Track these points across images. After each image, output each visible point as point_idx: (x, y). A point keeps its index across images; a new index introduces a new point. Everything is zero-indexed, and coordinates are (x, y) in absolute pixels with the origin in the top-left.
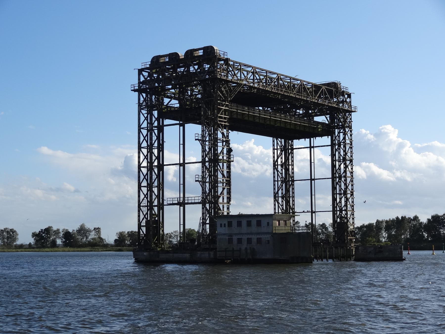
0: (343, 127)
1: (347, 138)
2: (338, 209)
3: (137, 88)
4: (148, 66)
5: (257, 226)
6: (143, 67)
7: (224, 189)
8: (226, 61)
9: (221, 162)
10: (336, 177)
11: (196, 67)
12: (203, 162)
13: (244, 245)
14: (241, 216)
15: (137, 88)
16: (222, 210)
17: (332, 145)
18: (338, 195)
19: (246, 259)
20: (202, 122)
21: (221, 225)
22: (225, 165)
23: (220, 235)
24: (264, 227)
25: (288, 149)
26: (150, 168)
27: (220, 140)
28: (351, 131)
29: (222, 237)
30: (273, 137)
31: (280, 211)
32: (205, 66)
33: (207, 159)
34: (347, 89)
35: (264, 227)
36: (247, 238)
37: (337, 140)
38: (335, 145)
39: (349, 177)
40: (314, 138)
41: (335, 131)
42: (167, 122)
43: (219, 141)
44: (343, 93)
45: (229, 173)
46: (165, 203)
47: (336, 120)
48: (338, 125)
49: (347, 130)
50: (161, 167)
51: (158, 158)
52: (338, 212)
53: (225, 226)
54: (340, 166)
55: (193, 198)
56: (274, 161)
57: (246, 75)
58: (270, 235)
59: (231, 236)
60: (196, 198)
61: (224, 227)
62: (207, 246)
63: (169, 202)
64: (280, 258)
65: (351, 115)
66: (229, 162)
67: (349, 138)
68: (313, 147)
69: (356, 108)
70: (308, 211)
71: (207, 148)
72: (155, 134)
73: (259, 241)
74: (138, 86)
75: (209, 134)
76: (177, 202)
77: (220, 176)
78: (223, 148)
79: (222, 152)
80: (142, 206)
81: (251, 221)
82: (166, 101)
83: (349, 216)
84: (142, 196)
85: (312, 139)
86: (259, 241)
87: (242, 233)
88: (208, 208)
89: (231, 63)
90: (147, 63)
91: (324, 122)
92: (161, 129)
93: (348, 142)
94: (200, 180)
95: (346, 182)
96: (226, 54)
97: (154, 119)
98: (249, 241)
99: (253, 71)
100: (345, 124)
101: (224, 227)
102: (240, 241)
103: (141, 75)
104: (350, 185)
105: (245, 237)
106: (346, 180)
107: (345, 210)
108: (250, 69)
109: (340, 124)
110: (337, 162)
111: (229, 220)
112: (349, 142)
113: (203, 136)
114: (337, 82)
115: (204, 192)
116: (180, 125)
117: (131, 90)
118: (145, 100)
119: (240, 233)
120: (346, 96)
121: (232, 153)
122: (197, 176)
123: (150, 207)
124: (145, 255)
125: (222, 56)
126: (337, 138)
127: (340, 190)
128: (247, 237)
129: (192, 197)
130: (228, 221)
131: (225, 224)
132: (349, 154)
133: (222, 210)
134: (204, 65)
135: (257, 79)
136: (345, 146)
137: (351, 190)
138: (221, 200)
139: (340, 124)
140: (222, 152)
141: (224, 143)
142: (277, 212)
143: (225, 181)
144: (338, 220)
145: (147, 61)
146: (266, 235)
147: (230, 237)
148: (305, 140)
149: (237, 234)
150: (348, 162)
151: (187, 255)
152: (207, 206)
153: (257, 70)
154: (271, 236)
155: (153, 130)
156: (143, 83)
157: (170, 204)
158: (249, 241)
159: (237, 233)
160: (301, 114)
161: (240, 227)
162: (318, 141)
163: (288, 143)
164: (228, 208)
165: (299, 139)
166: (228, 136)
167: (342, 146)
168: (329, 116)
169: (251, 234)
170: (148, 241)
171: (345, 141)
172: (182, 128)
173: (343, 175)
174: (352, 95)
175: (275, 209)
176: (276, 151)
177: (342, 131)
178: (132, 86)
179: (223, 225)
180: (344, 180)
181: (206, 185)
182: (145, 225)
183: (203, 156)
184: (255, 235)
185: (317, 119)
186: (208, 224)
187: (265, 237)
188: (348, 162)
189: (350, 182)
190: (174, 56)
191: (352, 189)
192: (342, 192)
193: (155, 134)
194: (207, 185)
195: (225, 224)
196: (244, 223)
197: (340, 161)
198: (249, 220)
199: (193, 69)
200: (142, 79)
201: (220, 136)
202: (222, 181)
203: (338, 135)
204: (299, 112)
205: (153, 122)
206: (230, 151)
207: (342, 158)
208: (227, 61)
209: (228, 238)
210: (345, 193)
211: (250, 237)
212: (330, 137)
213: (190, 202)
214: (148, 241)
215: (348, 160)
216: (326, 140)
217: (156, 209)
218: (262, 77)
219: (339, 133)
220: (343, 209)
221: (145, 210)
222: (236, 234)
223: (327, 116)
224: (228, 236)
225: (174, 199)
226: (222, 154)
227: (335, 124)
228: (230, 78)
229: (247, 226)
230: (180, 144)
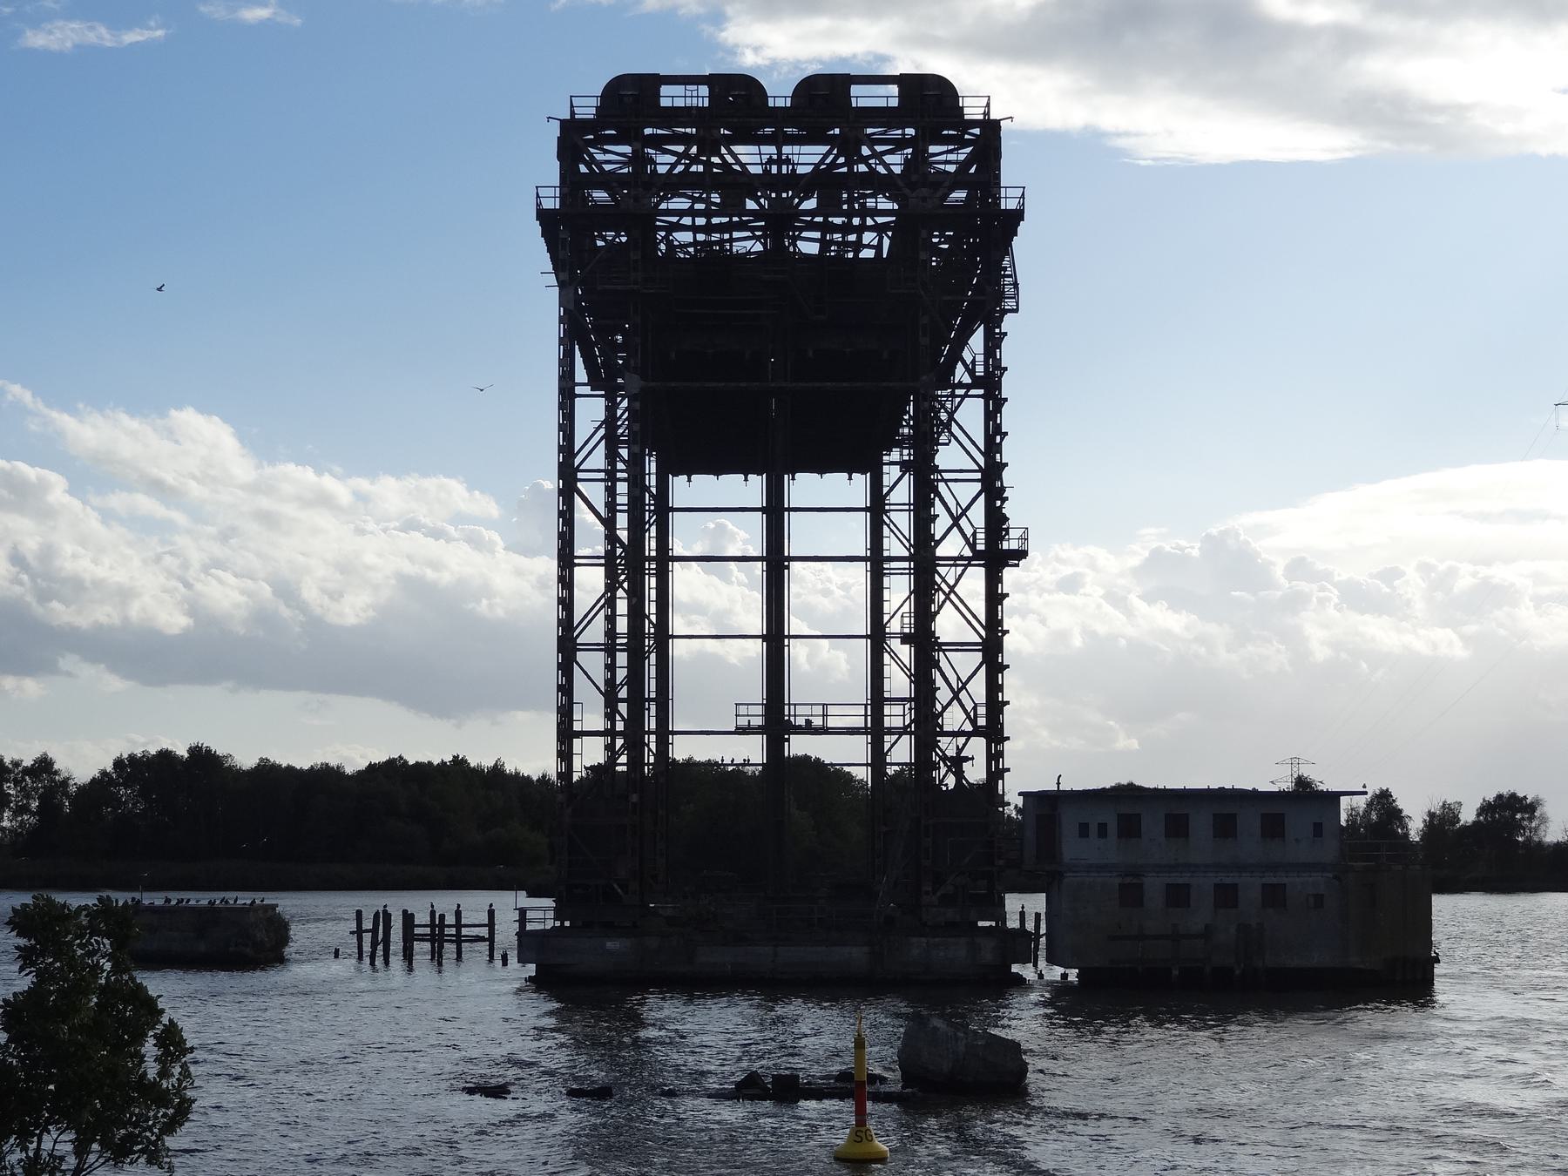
19: (1237, 972)
21: (1084, 830)
24: (1297, 840)
35: (1297, 840)
36: (1215, 884)
58: (1330, 875)
63: (743, 722)
64: (1362, 966)
70: (733, 760)
73: (1274, 896)
81: (1234, 816)
86: (1274, 896)
98: (1226, 896)
102: (1178, 896)
128: (1217, 881)
129: (812, 705)
131: (1103, 830)
147: (1128, 880)
151: (855, 954)
154: (1335, 877)
158: (1226, 896)
165: (717, 473)
170: (619, 890)
179: (1093, 829)
184: (1254, 875)
196: (1201, 824)
211: (1228, 881)
214: (616, 886)
229: (1215, 837)
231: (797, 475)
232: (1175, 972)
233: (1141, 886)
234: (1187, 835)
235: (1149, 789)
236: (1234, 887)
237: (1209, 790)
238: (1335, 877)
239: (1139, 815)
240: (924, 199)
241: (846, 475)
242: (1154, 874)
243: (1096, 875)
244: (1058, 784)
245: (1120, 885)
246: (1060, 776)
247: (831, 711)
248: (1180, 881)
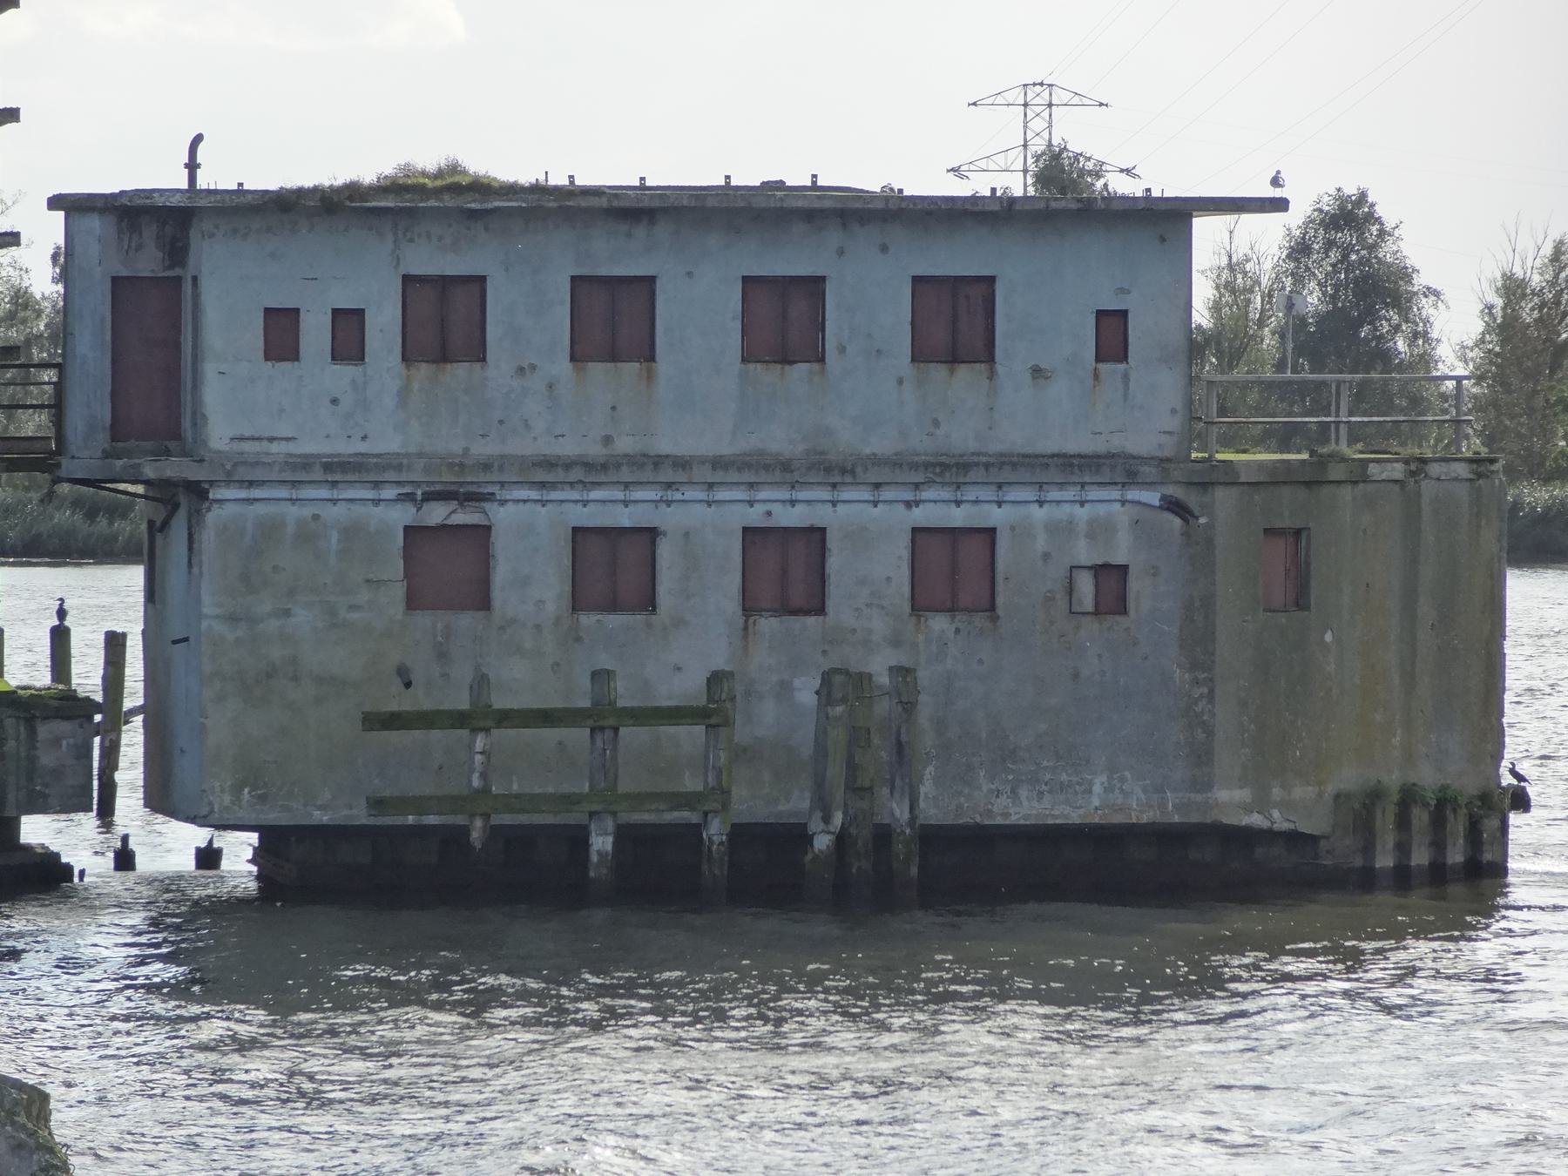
19: (822, 842)
23: (251, 484)
24: (1037, 372)
29: (307, 511)
35: (1037, 372)
36: (750, 534)
58: (1153, 497)
61: (337, 356)
64: (1256, 820)
81: (815, 286)
87: (658, 461)
101: (337, 356)
111: (428, 260)
119: (624, 445)
128: (755, 516)
130: (407, 279)
146: (1070, 493)
147: (437, 514)
159: (568, 448)
179: (315, 333)
184: (887, 494)
224: (409, 497)
232: (602, 842)
233: (482, 533)
234: (648, 355)
235: (512, 190)
237: (727, 189)
238: (1174, 506)
239: (478, 282)
242: (534, 495)
243: (324, 493)
244: (192, 166)
245: (407, 529)
246: (198, 139)
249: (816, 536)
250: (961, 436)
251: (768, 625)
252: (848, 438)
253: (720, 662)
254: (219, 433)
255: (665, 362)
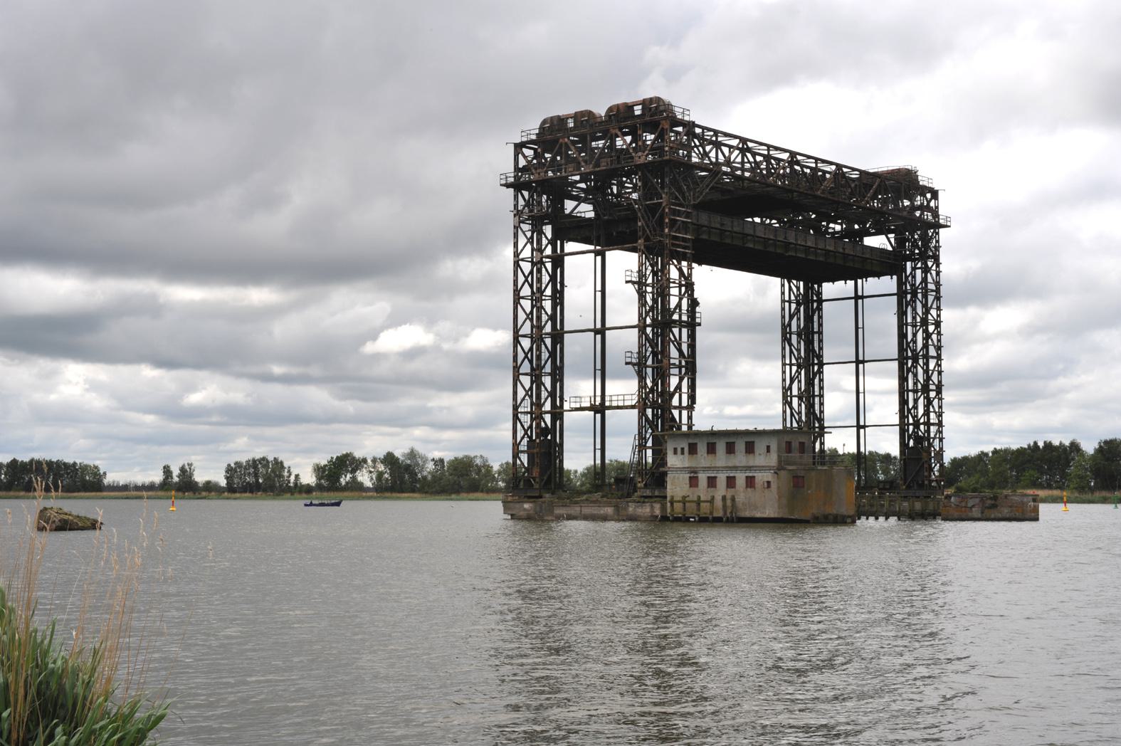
0: (924, 257)
1: (930, 279)
2: (911, 421)
3: (512, 180)
4: (534, 137)
5: (746, 452)
6: (524, 139)
7: (681, 379)
8: (687, 128)
9: (676, 327)
10: (908, 358)
11: (628, 139)
12: (641, 327)
13: (721, 489)
14: (712, 434)
15: (512, 180)
16: (678, 420)
17: (901, 294)
18: (911, 394)
20: (639, 247)
21: (675, 452)
22: (685, 331)
24: (760, 454)
25: (813, 301)
26: (537, 338)
27: (674, 283)
28: (938, 266)
30: (782, 277)
31: (795, 425)
32: (646, 136)
33: (648, 321)
34: (930, 181)
36: (727, 477)
37: (909, 282)
38: (906, 293)
39: (933, 357)
40: (864, 279)
41: (905, 265)
42: (570, 246)
43: (672, 285)
44: (924, 190)
45: (692, 346)
46: (566, 406)
47: (907, 244)
48: (913, 253)
49: (930, 264)
50: (558, 337)
51: (552, 318)
52: (911, 428)
53: (683, 453)
54: (915, 335)
55: (621, 398)
56: (783, 324)
57: (727, 154)
58: (773, 471)
59: (695, 472)
60: (626, 397)
62: (648, 493)
63: (573, 405)
65: (938, 233)
66: (692, 325)
67: (933, 280)
68: (863, 297)
69: (949, 219)
71: (649, 298)
72: (547, 270)
73: (750, 482)
74: (515, 177)
75: (652, 271)
76: (588, 405)
77: (674, 352)
78: (681, 299)
79: (679, 305)
80: (521, 413)
81: (734, 443)
82: (569, 205)
83: (932, 435)
84: (521, 393)
85: (859, 281)
86: (750, 482)
88: (650, 417)
89: (698, 131)
90: (532, 132)
91: (883, 247)
92: (558, 261)
93: (931, 286)
94: (634, 361)
95: (928, 367)
96: (687, 113)
97: (544, 241)
98: (731, 482)
99: (740, 146)
100: (926, 251)
102: (712, 482)
103: (520, 155)
104: (936, 373)
105: (722, 478)
106: (927, 364)
107: (924, 423)
108: (735, 142)
109: (917, 251)
110: (909, 328)
111: (691, 441)
112: (934, 288)
113: (641, 274)
114: (910, 168)
115: (642, 386)
116: (597, 253)
117: (501, 185)
118: (527, 204)
119: (713, 465)
120: (929, 196)
121: (698, 309)
122: (629, 355)
123: (537, 415)
124: (525, 510)
125: (680, 117)
126: (910, 278)
127: (915, 384)
128: (727, 475)
131: (683, 449)
132: (934, 312)
133: (678, 420)
134: (644, 134)
135: (749, 162)
136: (925, 296)
137: (936, 383)
138: (675, 402)
139: (917, 251)
140: (679, 305)
141: (683, 289)
142: (789, 425)
143: (683, 363)
144: (911, 443)
145: (532, 127)
147: (692, 475)
148: (846, 283)
149: (705, 468)
150: (931, 328)
152: (649, 412)
153: (750, 145)
155: (543, 264)
156: (524, 170)
157: (577, 409)
158: (731, 482)
160: (838, 232)
161: (713, 455)
162: (872, 285)
163: (812, 288)
164: (690, 418)
166: (690, 275)
167: (920, 296)
168: (893, 235)
169: (735, 468)
171: (926, 285)
172: (599, 258)
173: (921, 353)
174: (941, 195)
175: (785, 420)
176: (787, 304)
177: (919, 265)
178: (502, 177)
180: (924, 364)
181: (646, 373)
182: (526, 448)
183: (640, 315)
185: (871, 241)
186: (649, 448)
187: (761, 477)
188: (931, 328)
189: (935, 367)
190: (585, 118)
191: (940, 382)
192: (920, 387)
193: (547, 270)
194: (649, 371)
195: (683, 449)
197: (916, 326)
198: (731, 440)
199: (621, 143)
200: (522, 163)
201: (674, 273)
202: (677, 363)
203: (911, 273)
204: (834, 229)
205: (543, 247)
206: (694, 303)
207: (918, 319)
208: (689, 126)
209: (690, 477)
210: (926, 389)
211: (731, 475)
212: (895, 277)
213: (614, 404)
215: (933, 324)
216: (888, 283)
217: (548, 418)
218: (759, 158)
219: (914, 269)
220: (922, 421)
221: (526, 419)
222: (706, 469)
223: (890, 236)
225: (583, 400)
226: (678, 311)
227: (905, 252)
228: (695, 160)
229: (727, 453)
230: (595, 291)
231: (868, 279)
233: (697, 477)
234: (715, 453)
236: (715, 477)
238: (775, 473)
240: (640, 157)
241: (890, 277)
247: (614, 398)
248: (713, 475)
249: (734, 477)
250: (751, 464)
251: (729, 489)
252: (738, 464)
253: (724, 494)
254: (669, 465)
255: (717, 454)
